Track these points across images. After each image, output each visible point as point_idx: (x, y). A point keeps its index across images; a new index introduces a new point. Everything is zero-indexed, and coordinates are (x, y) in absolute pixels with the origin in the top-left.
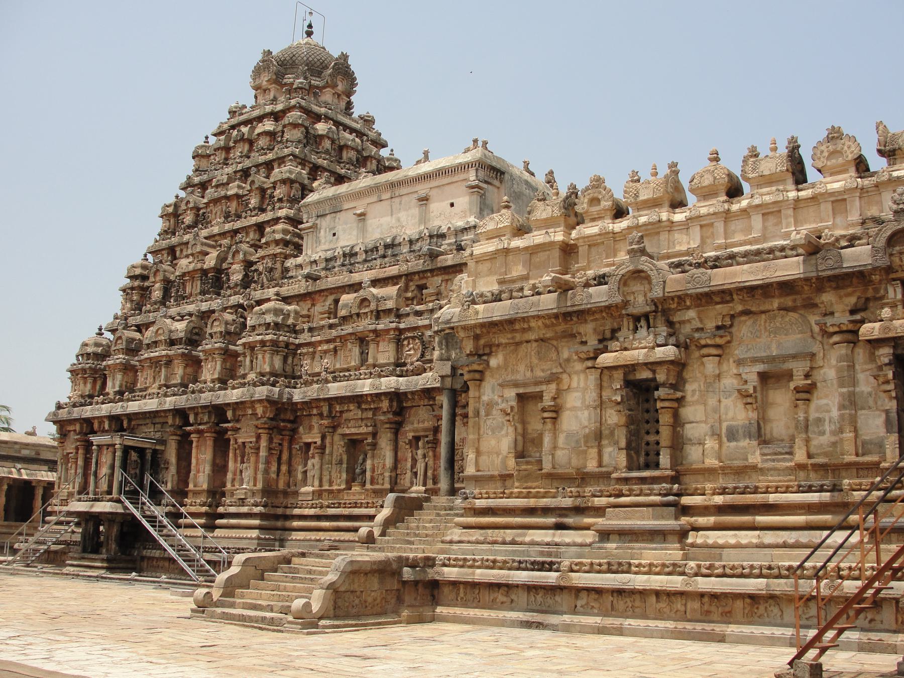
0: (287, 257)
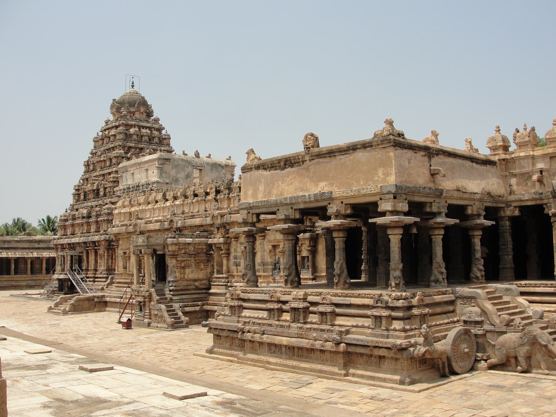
0: (114, 187)
